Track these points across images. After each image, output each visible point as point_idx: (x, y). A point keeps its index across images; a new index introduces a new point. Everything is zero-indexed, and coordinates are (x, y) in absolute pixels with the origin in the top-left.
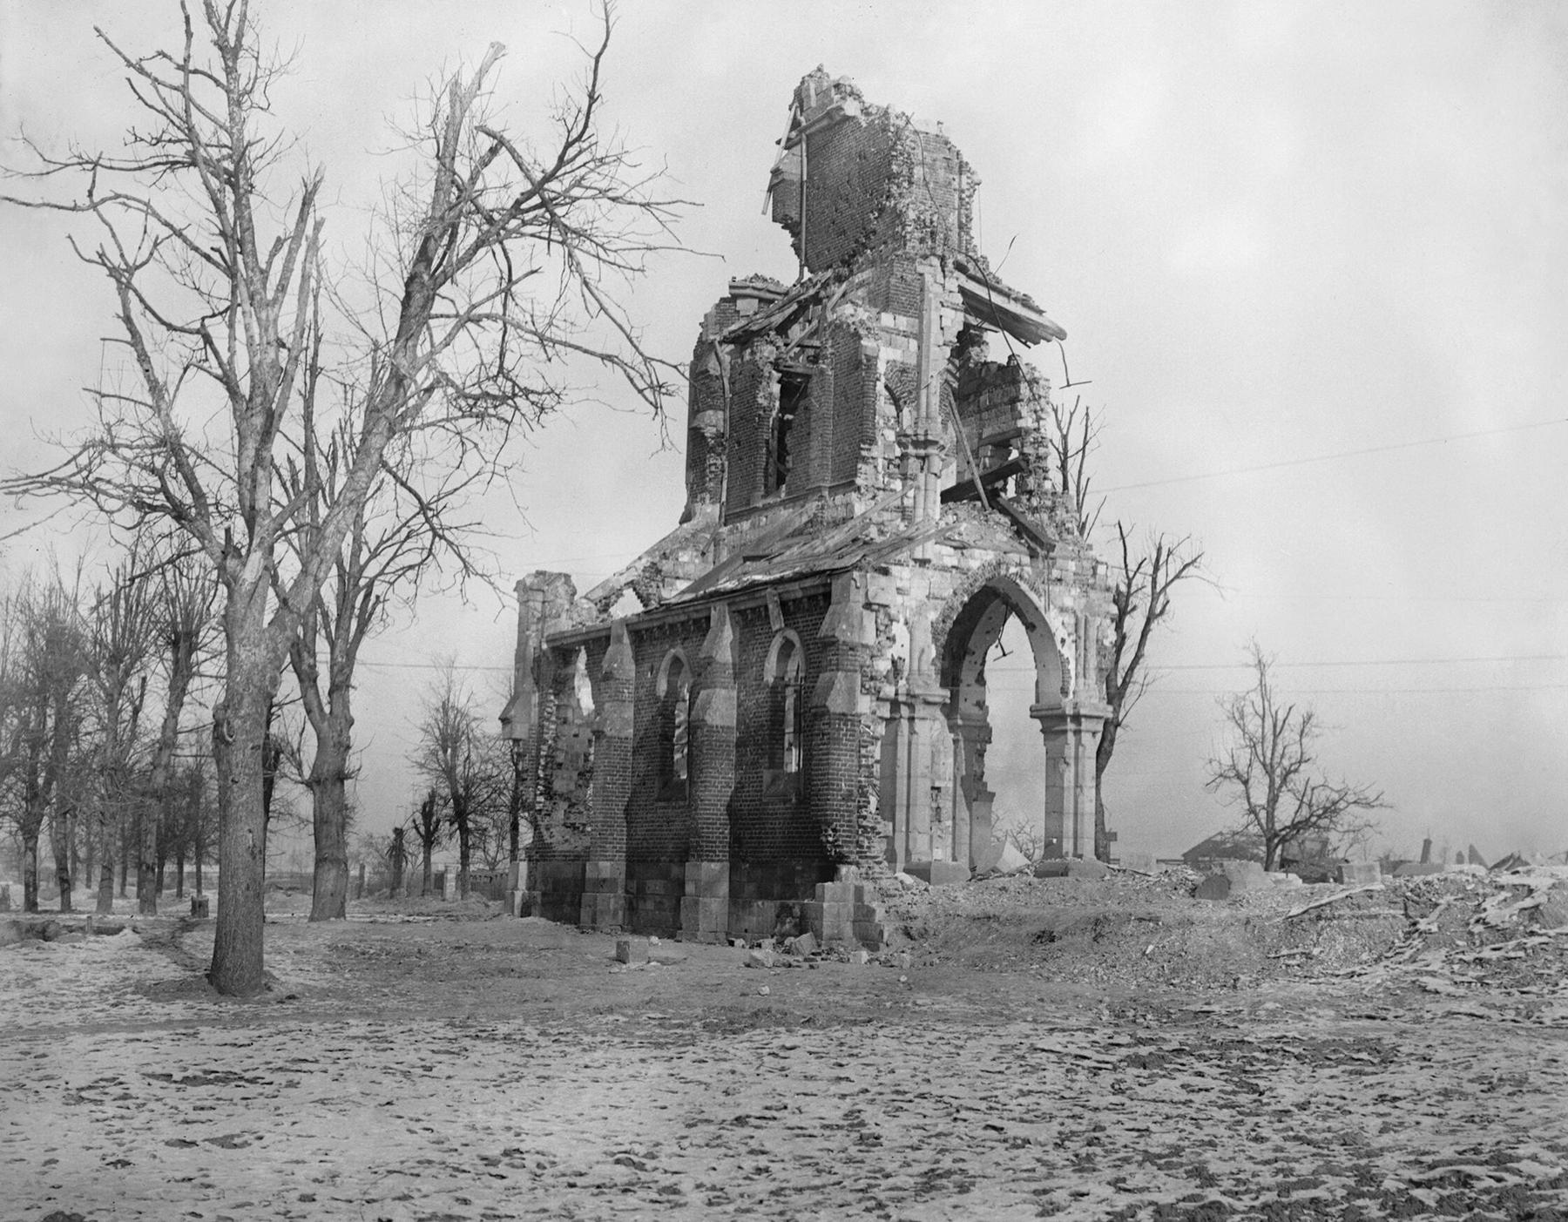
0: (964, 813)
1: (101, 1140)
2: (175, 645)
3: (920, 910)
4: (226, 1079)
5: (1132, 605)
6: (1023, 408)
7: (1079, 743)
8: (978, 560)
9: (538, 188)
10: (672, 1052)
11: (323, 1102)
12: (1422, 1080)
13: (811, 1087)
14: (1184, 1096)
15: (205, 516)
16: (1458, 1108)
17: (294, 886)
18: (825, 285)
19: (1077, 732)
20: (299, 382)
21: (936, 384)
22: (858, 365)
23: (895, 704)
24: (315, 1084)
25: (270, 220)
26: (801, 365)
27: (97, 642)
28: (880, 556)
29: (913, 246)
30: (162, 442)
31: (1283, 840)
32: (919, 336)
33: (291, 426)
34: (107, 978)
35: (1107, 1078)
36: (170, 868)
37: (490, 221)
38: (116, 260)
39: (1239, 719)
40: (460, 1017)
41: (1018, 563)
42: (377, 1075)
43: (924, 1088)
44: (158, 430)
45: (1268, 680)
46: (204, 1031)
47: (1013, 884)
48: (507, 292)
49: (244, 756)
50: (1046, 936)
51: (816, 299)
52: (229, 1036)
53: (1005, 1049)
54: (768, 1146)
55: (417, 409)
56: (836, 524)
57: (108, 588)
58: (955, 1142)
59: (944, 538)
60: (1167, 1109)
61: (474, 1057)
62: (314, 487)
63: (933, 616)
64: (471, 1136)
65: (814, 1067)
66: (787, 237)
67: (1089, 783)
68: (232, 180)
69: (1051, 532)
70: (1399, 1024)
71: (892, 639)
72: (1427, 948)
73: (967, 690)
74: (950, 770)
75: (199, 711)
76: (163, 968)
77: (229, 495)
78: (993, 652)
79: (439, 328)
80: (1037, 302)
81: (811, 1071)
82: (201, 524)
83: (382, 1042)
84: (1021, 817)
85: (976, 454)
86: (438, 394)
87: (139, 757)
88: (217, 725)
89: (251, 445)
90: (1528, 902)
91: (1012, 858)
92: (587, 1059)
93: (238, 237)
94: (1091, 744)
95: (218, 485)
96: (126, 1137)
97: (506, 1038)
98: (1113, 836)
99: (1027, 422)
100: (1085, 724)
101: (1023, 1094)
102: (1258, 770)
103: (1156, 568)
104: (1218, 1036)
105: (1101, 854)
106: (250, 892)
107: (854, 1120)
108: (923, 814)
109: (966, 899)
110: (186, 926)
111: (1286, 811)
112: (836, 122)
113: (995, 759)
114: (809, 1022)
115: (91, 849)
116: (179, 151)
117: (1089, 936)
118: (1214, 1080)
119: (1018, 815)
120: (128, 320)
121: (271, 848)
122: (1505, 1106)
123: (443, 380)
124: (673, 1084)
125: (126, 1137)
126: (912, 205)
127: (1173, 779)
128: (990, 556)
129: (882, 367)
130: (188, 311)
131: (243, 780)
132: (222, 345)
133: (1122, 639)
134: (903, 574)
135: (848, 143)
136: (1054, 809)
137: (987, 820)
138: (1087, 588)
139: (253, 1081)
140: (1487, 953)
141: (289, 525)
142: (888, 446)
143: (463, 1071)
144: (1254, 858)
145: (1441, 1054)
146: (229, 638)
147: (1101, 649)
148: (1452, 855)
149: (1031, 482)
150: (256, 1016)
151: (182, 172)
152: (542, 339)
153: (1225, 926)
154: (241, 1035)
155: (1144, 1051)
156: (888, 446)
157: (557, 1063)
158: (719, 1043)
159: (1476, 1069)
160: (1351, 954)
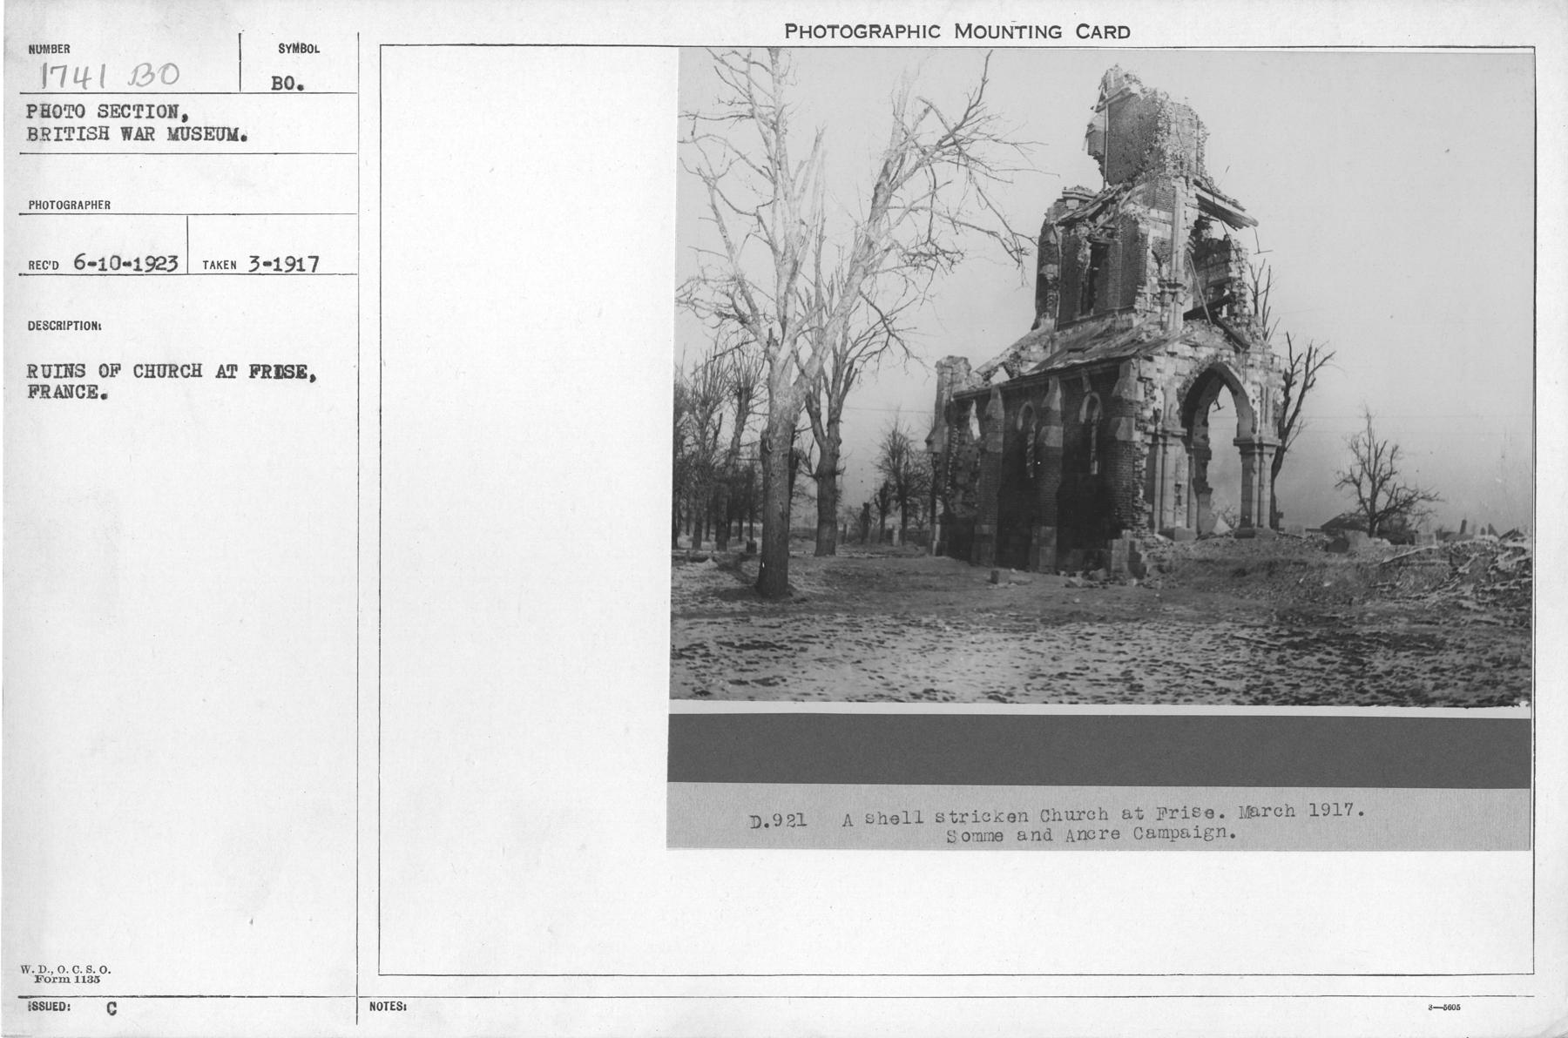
0: (1194, 500)
1: (692, 680)
2: (739, 395)
3: (1168, 556)
4: (766, 646)
5: (1295, 380)
6: (1232, 266)
7: (1262, 460)
8: (1204, 353)
9: (952, 134)
10: (1023, 635)
11: (821, 660)
12: (1459, 660)
13: (1103, 656)
14: (1319, 666)
15: (757, 321)
16: (1479, 676)
17: (806, 535)
18: (1118, 192)
19: (1261, 454)
20: (813, 242)
21: (1182, 251)
22: (1136, 239)
23: (1155, 436)
24: (817, 650)
25: (796, 147)
26: (1103, 239)
27: (694, 393)
28: (1147, 350)
29: (1170, 171)
30: (734, 279)
31: (1381, 519)
32: (1172, 223)
33: (807, 269)
34: (697, 587)
35: (1275, 655)
36: (734, 524)
37: (924, 152)
38: (708, 173)
39: (1355, 448)
40: (900, 613)
41: (1228, 355)
42: (852, 645)
43: (1169, 659)
44: (732, 273)
45: (1373, 426)
46: (753, 619)
47: (1222, 542)
48: (933, 195)
49: (777, 460)
50: (1241, 573)
51: (1113, 201)
52: (767, 622)
53: (1216, 637)
54: (1078, 690)
55: (881, 261)
56: (1123, 331)
57: (701, 362)
58: (1185, 690)
59: (1185, 340)
60: (1309, 673)
61: (908, 636)
62: (821, 306)
63: (1178, 385)
64: (906, 682)
65: (1105, 645)
66: (1096, 164)
67: (1267, 484)
68: (775, 126)
69: (1247, 338)
70: (1446, 627)
71: (1154, 398)
72: (1463, 583)
73: (1198, 430)
74: (1186, 476)
75: (751, 435)
76: (729, 581)
77: (772, 310)
78: (1213, 407)
79: (894, 215)
80: (1241, 204)
81: (1103, 647)
82: (755, 326)
83: (854, 627)
84: (1227, 503)
85: (1204, 292)
86: (892, 252)
87: (718, 459)
88: (763, 442)
89: (785, 280)
90: (1522, 558)
91: (1222, 527)
92: (973, 638)
93: (778, 161)
94: (1269, 461)
95: (766, 306)
96: (707, 678)
97: (927, 626)
98: (1281, 515)
99: (1234, 274)
100: (1266, 450)
101: (1226, 663)
102: (1366, 478)
103: (1308, 359)
104: (1340, 632)
105: (1274, 524)
106: (780, 538)
107: (1127, 676)
108: (1170, 501)
109: (1194, 550)
110: (743, 557)
111: (1382, 502)
112: (1126, 97)
113: (1213, 469)
114: (1102, 619)
115: (689, 512)
116: (744, 110)
117: (1265, 573)
118: (1337, 658)
119: (1226, 500)
120: (714, 207)
121: (793, 514)
122: (1507, 676)
123: (896, 244)
124: (1024, 654)
125: (707, 678)
126: (1170, 145)
127: (1317, 480)
128: (1212, 351)
129: (1150, 241)
130: (748, 203)
131: (778, 474)
132: (767, 222)
133: (1288, 400)
134: (1161, 361)
135: (1132, 110)
136: (1247, 499)
137: (1207, 504)
138: (1268, 370)
139: (781, 647)
140: (1498, 587)
141: (806, 327)
142: (1153, 287)
143: (902, 645)
144: (1363, 529)
145: (1470, 645)
146: (770, 392)
147: (1276, 407)
148: (1478, 530)
149: (1236, 309)
150: (783, 610)
151: (746, 121)
152: (953, 222)
153: (1345, 568)
154: (774, 621)
155: (1297, 639)
156: (1153, 287)
157: (956, 641)
158: (1050, 631)
159: (1490, 654)
160: (1418, 587)
